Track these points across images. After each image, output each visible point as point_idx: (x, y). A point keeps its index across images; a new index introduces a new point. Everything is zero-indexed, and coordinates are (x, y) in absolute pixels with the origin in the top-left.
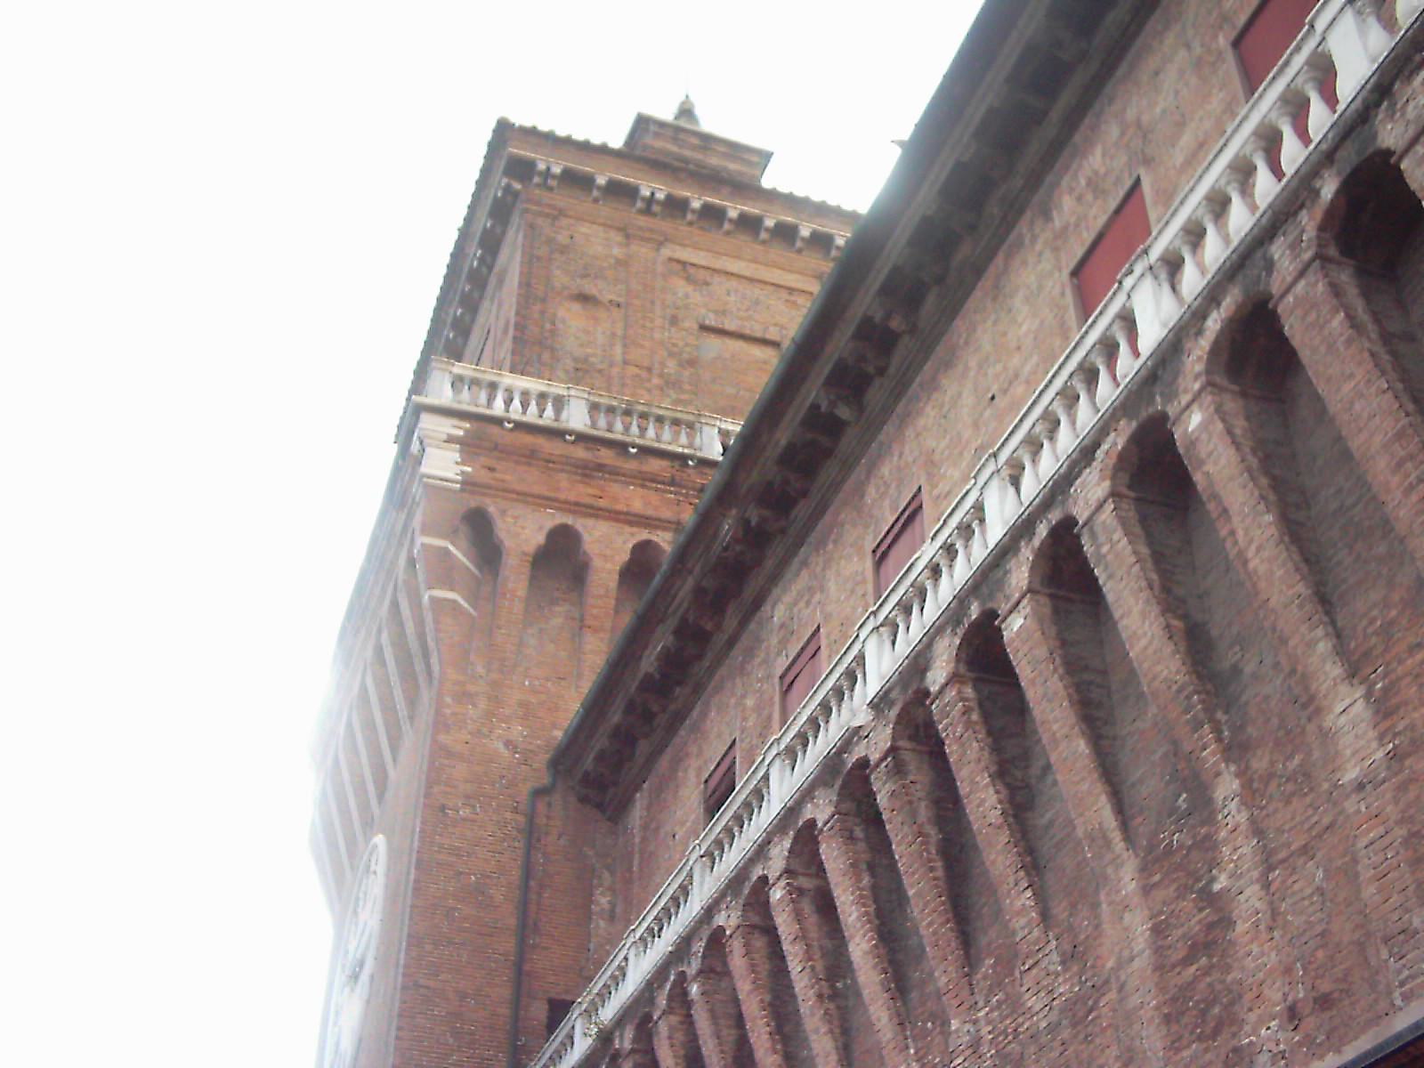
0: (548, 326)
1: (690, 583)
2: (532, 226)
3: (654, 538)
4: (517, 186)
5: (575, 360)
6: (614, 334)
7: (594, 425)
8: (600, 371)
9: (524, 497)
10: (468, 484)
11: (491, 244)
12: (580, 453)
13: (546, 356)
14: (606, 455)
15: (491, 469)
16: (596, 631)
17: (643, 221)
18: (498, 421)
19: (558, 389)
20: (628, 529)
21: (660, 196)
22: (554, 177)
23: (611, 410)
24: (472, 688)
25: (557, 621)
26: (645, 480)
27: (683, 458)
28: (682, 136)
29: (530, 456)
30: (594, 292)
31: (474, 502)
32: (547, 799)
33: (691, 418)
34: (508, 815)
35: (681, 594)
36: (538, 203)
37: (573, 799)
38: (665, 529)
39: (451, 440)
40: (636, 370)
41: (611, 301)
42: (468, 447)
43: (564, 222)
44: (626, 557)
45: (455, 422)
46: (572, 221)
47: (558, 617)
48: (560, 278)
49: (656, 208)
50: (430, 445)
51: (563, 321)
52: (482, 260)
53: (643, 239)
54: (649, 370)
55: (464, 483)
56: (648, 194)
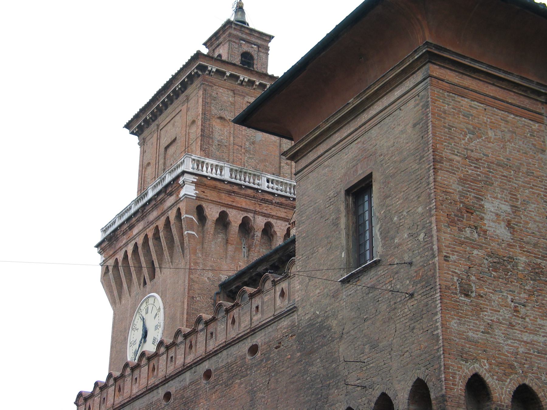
0: (211, 130)
1: (278, 256)
2: (205, 90)
3: (248, 216)
4: (200, 73)
5: (218, 141)
6: (230, 132)
7: (231, 177)
8: (226, 146)
9: (213, 202)
10: (198, 198)
11: (184, 86)
12: (228, 187)
13: (210, 141)
14: (235, 188)
15: (204, 192)
16: (232, 244)
17: (240, 88)
18: (206, 177)
19: (221, 164)
20: (241, 212)
21: (246, 80)
22: (213, 72)
23: (236, 170)
24: (198, 261)
25: (219, 240)
26: (246, 196)
27: (257, 190)
28: (243, 29)
29: (215, 188)
30: (224, 116)
31: (199, 203)
32: (219, 295)
33: (259, 174)
34: (209, 300)
35: (274, 258)
36: (207, 81)
37: (226, 296)
38: (251, 213)
39: (193, 182)
40: (237, 147)
41: (229, 120)
42: (197, 185)
43: (215, 87)
44: (240, 222)
45: (194, 177)
46: (217, 87)
47: (220, 237)
48: (214, 111)
49: (244, 83)
50: (187, 184)
51: (215, 127)
52: (180, 89)
53: (239, 95)
54: (241, 147)
55: (197, 197)
56: (242, 79)
